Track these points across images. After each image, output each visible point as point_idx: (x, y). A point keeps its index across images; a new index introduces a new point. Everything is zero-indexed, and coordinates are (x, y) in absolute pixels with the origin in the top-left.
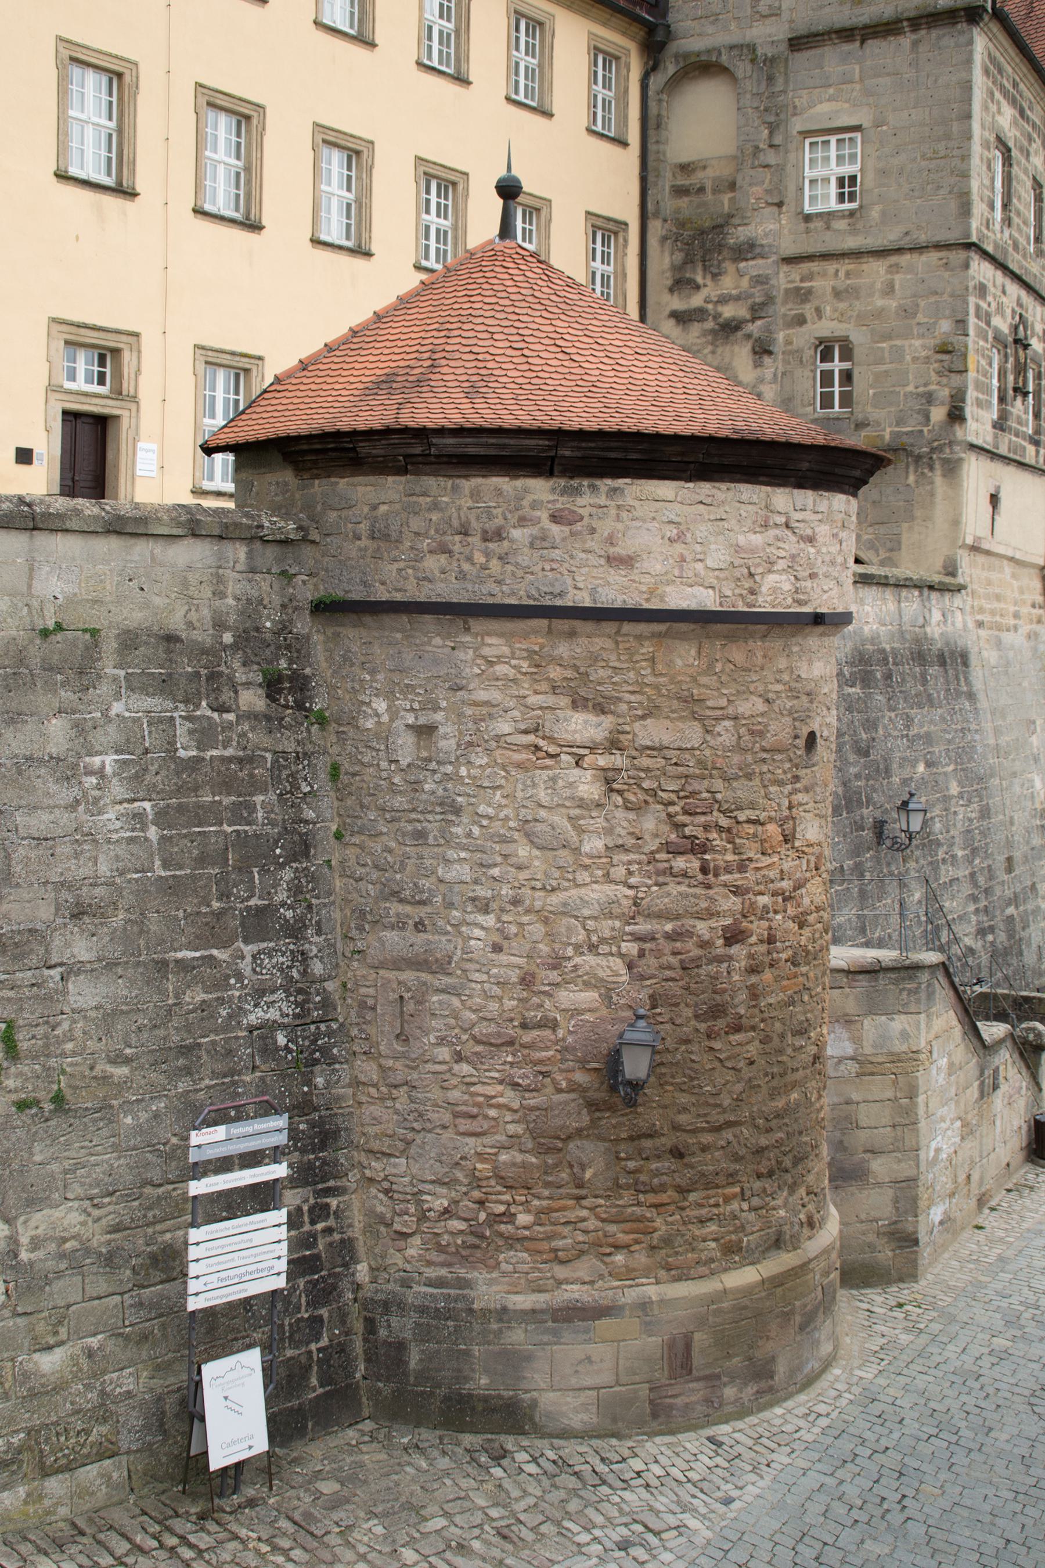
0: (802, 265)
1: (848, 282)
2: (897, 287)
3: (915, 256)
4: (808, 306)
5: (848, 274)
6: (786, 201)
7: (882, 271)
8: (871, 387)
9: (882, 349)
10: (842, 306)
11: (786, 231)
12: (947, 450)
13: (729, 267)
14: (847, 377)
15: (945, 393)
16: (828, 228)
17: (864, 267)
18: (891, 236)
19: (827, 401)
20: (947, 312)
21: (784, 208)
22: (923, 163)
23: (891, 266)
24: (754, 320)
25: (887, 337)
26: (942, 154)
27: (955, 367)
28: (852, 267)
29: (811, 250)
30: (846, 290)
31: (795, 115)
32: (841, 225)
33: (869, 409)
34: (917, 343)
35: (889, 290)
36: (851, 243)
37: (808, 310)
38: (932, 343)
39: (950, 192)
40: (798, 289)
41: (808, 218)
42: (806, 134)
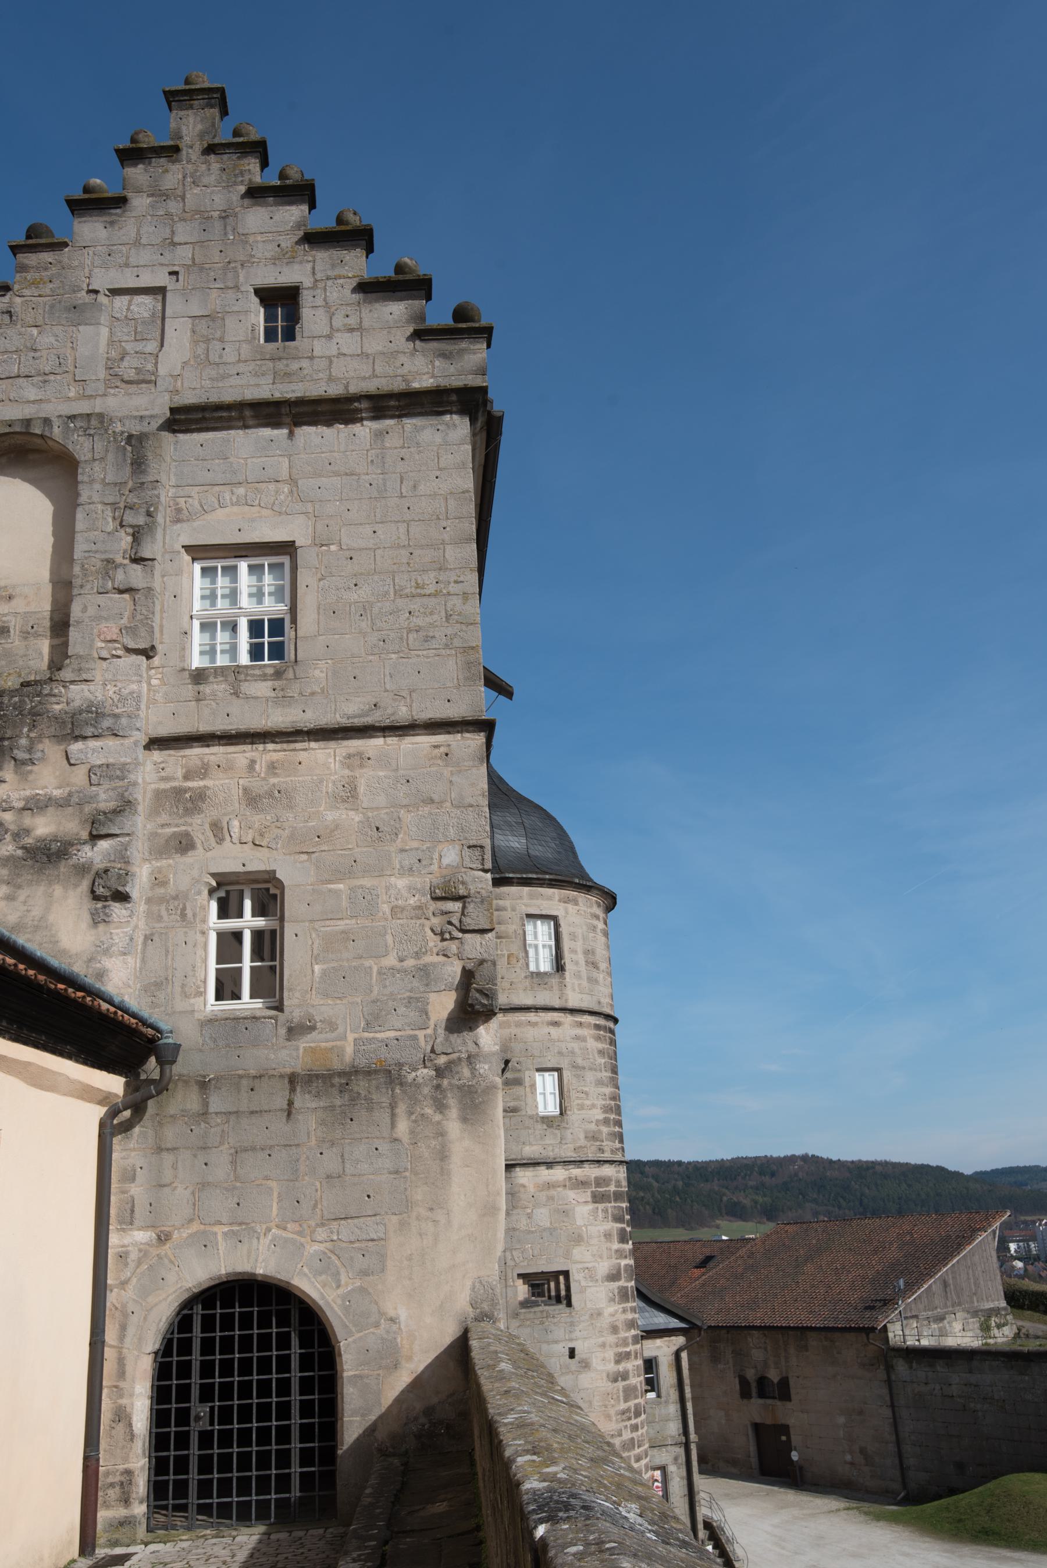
0: (188, 752)
1: (274, 780)
2: (362, 789)
3: (392, 741)
4: (197, 819)
5: (272, 767)
6: (160, 648)
7: (335, 765)
8: (316, 959)
9: (337, 893)
10: (257, 819)
11: (159, 697)
12: (466, 1072)
13: (51, 750)
14: (267, 945)
15: (454, 970)
16: (236, 694)
17: (302, 756)
18: (348, 710)
19: (227, 988)
20: (452, 832)
21: (156, 661)
22: (400, 602)
23: (349, 756)
24: (94, 838)
25: (339, 875)
26: (431, 589)
27: (470, 923)
28: (275, 756)
29: (204, 728)
30: (270, 795)
31: (178, 521)
32: (262, 689)
33: (316, 999)
34: (401, 883)
35: (349, 795)
36: (279, 719)
37: (198, 826)
38: (424, 881)
39: (446, 646)
40: (179, 792)
41: (199, 676)
42: (197, 552)
